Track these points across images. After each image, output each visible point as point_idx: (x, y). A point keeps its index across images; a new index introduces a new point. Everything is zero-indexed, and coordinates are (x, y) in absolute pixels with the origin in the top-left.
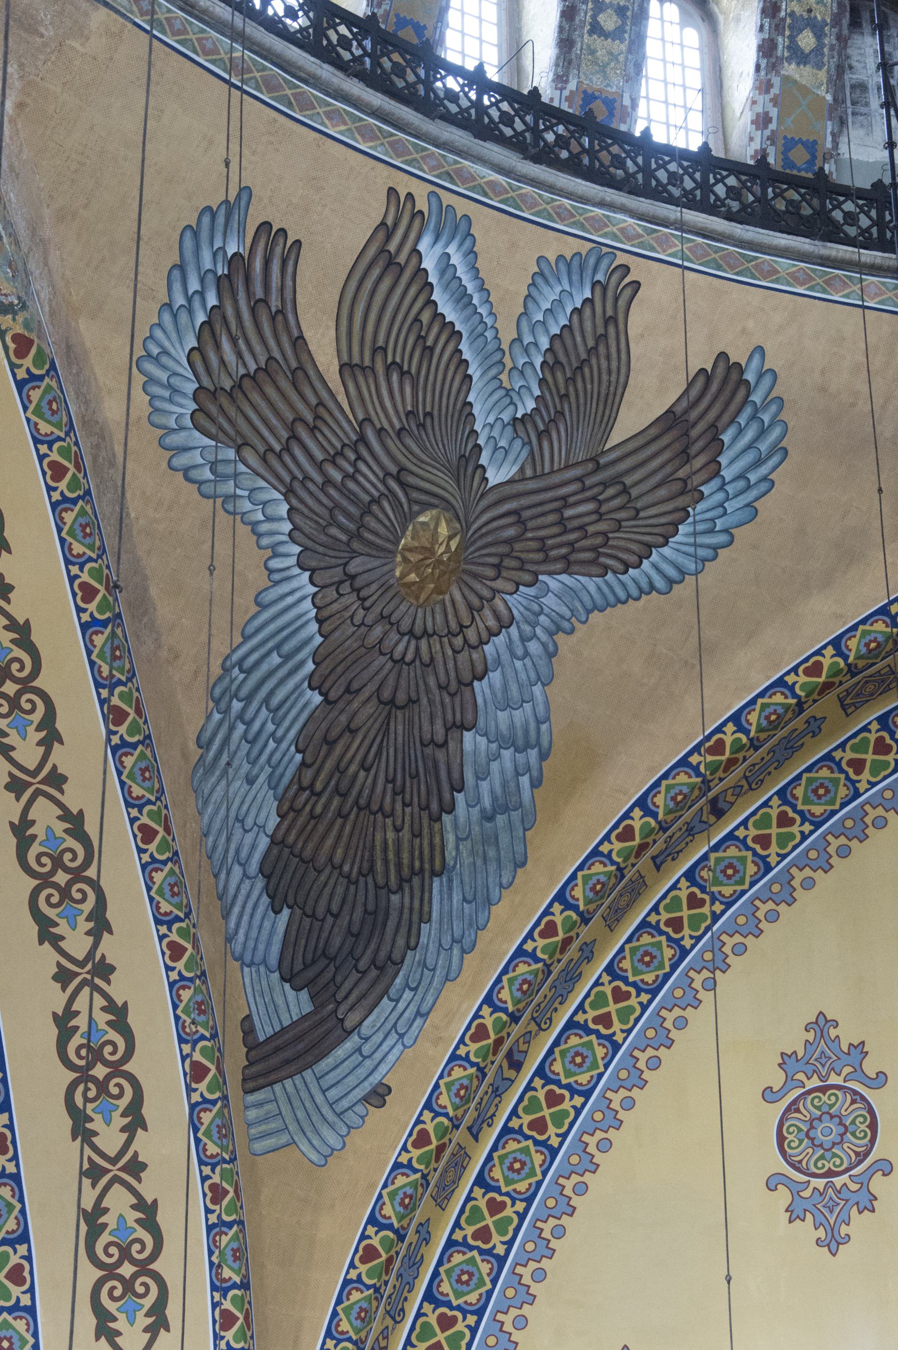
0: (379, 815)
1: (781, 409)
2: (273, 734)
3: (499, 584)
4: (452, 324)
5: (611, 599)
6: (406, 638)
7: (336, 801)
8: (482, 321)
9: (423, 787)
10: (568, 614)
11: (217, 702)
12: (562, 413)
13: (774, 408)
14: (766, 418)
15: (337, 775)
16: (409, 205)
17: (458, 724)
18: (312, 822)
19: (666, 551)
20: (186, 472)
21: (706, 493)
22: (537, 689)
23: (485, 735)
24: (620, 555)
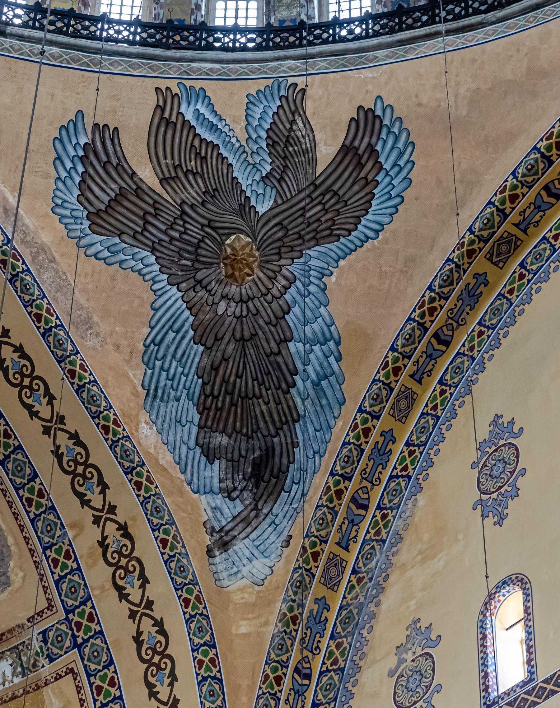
0: (254, 399)
1: (401, 123)
2: (182, 373)
3: (283, 262)
4: (211, 142)
5: (347, 251)
6: (240, 304)
7: (228, 398)
8: (227, 135)
9: (274, 378)
10: (326, 266)
11: (147, 364)
12: (287, 166)
13: (398, 124)
14: (396, 130)
15: (224, 384)
16: (169, 93)
17: (283, 339)
18: (219, 413)
19: (369, 217)
20: (95, 255)
22: (322, 310)
23: (301, 341)
24: (344, 227)
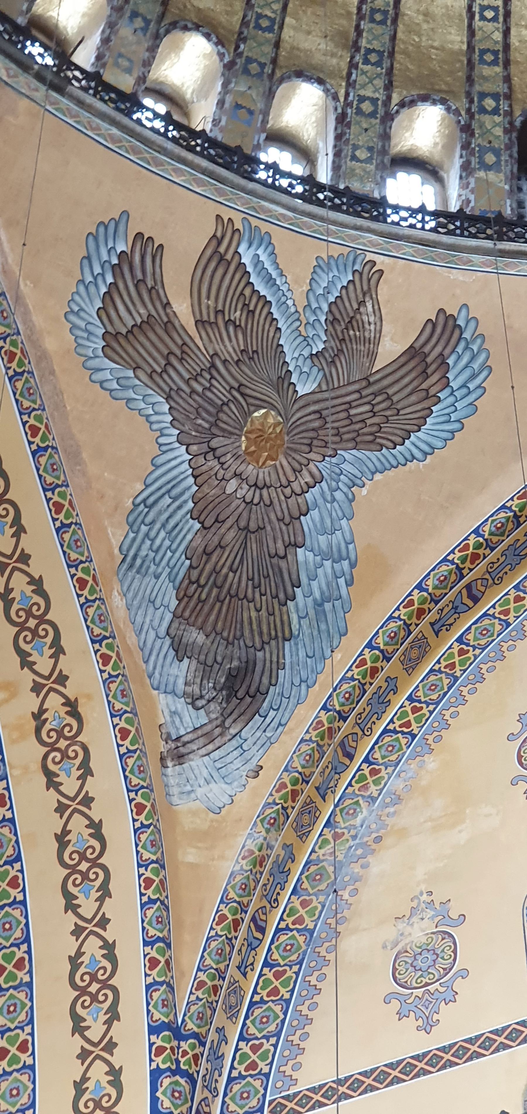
0: (245, 600)
1: (483, 341)
2: (169, 547)
3: (312, 456)
4: (265, 296)
5: (388, 466)
6: (253, 488)
7: (215, 591)
8: (284, 295)
9: (273, 584)
10: (359, 475)
11: (131, 527)
12: (342, 351)
13: (479, 341)
14: (475, 348)
15: (214, 575)
16: (230, 226)
17: (293, 543)
18: (200, 605)
20: (101, 383)
21: (442, 398)
22: (344, 522)
23: (312, 551)
24: (390, 437)
